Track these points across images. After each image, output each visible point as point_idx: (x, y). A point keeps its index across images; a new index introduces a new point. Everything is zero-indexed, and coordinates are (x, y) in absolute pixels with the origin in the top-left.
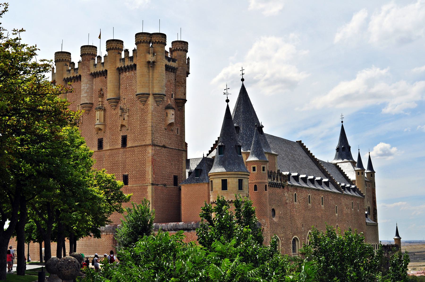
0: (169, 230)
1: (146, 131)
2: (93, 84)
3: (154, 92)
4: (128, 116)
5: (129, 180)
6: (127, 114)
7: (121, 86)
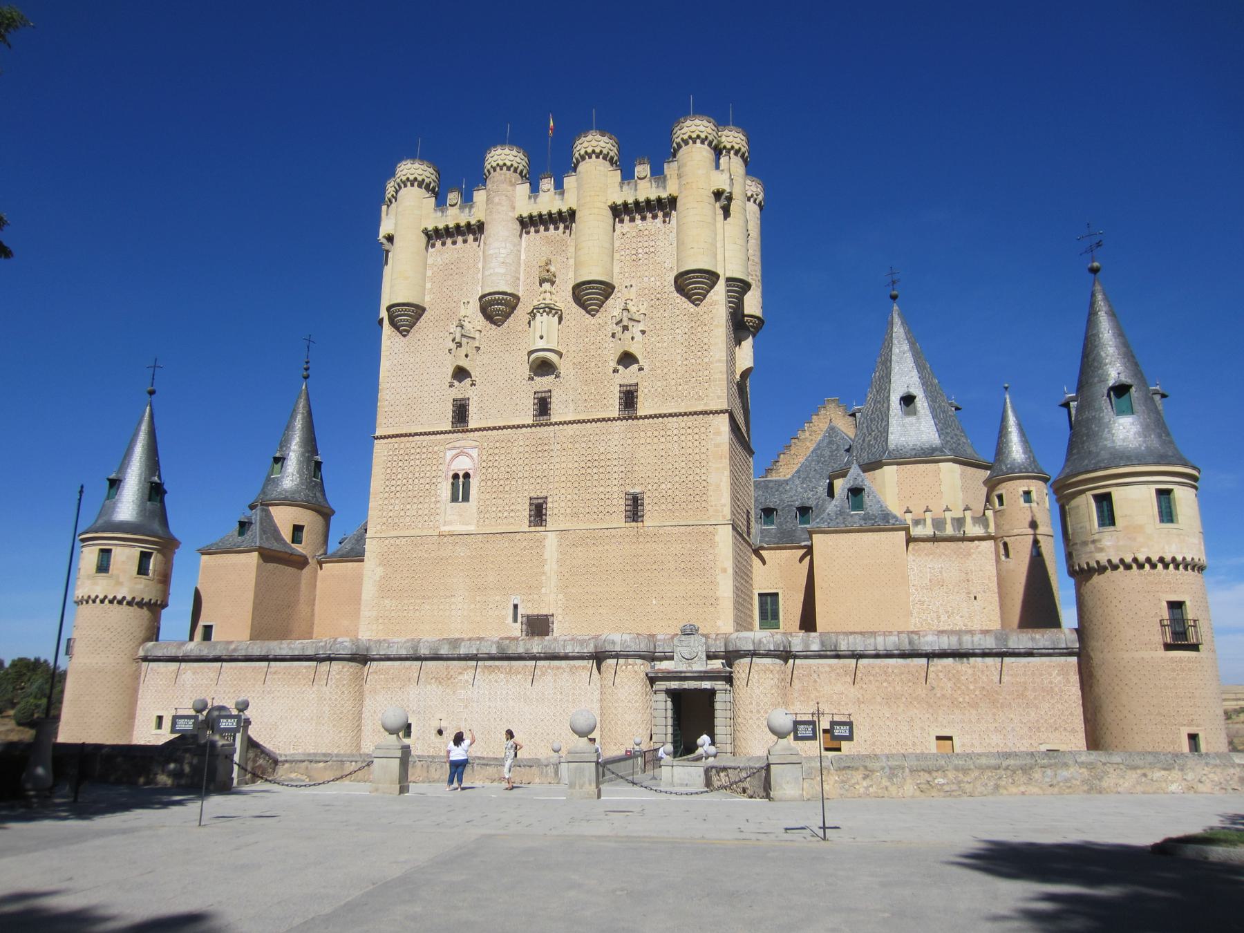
0: (877, 656)
1: (706, 373)
2: (520, 244)
3: (729, 275)
4: (643, 332)
5: (647, 508)
6: (641, 327)
7: (617, 256)
